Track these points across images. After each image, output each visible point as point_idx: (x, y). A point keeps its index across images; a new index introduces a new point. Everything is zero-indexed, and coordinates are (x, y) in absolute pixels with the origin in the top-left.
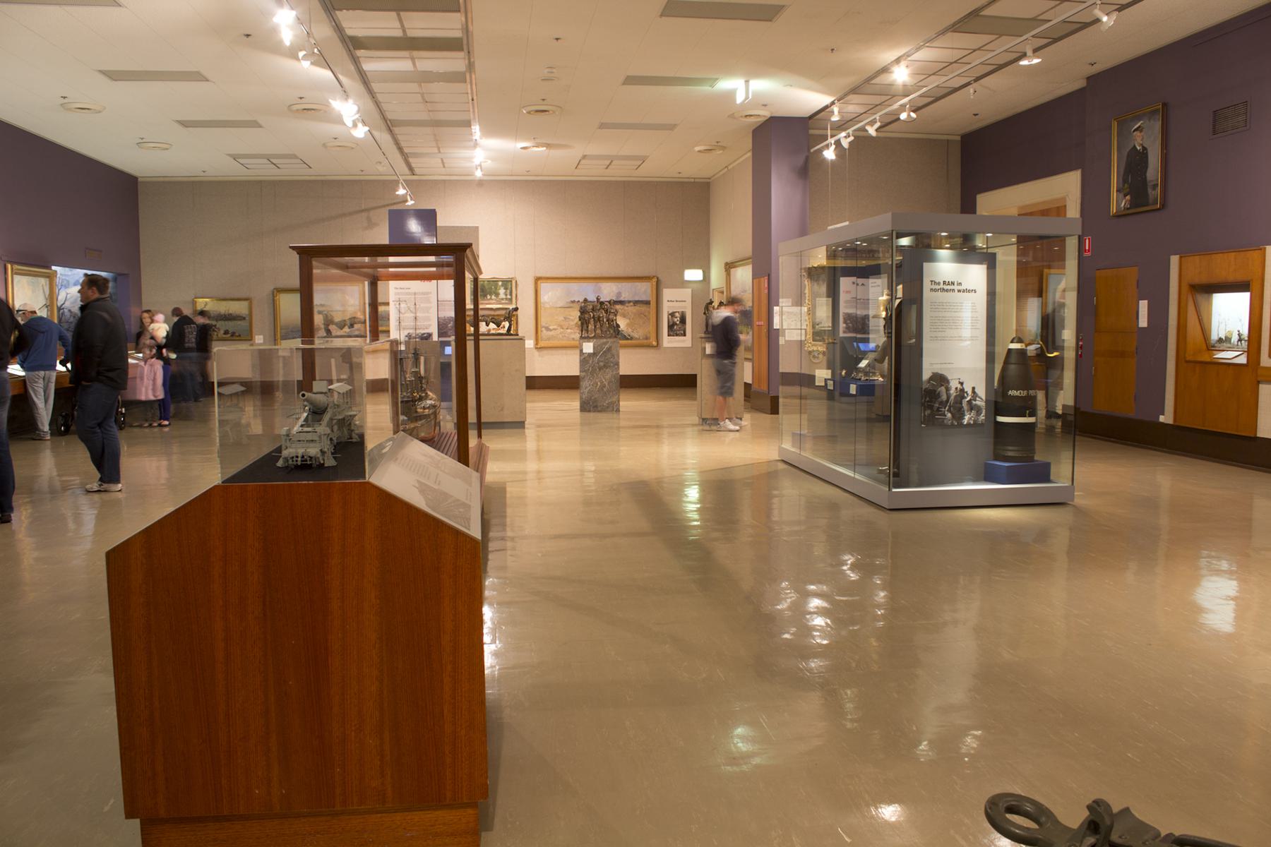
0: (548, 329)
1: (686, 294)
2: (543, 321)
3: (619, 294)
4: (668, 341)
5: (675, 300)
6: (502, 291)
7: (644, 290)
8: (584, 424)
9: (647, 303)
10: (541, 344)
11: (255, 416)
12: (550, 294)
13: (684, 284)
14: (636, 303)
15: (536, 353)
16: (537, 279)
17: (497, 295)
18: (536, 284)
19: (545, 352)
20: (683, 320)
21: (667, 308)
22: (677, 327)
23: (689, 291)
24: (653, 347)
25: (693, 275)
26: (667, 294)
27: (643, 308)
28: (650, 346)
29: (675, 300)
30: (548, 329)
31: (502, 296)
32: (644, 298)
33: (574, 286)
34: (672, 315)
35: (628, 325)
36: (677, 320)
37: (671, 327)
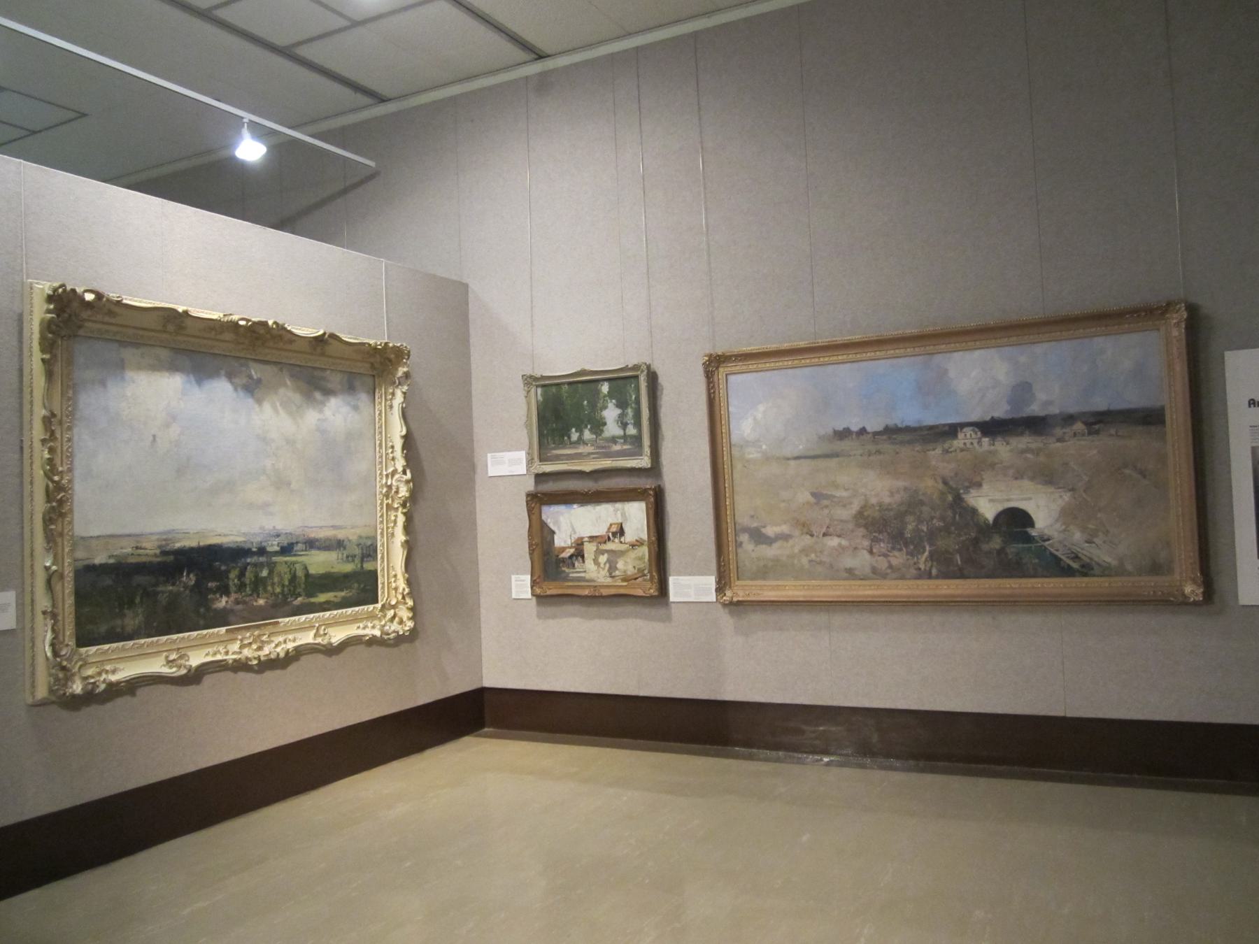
0: (759, 537)
2: (744, 507)
3: (1022, 390)
6: (611, 413)
9: (1151, 418)
10: (740, 591)
12: (764, 413)
14: (1098, 421)
15: (726, 620)
16: (714, 364)
17: (598, 426)
18: (709, 375)
19: (756, 617)
24: (1183, 604)
27: (1134, 442)
28: (1170, 603)
30: (759, 537)
31: (612, 429)
32: (1133, 398)
33: (845, 375)
35: (1068, 515)
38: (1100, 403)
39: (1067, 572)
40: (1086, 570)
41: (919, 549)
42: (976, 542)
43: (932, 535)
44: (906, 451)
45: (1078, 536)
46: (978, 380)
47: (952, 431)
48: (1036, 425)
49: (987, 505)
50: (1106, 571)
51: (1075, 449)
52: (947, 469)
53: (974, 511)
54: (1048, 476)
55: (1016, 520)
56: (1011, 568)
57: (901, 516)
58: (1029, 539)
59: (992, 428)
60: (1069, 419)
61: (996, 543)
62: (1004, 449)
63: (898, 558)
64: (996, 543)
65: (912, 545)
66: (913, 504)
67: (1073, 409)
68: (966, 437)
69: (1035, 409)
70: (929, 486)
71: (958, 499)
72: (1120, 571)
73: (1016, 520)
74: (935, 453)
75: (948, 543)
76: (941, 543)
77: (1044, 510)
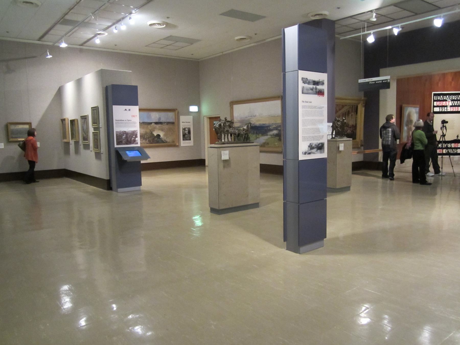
1: (190, 118)
3: (160, 118)
4: (183, 143)
5: (185, 121)
7: (170, 116)
8: (261, 176)
9: (173, 123)
11: (437, 132)
13: (189, 113)
14: (168, 123)
20: (189, 132)
21: (182, 126)
22: (186, 137)
23: (191, 117)
25: (194, 109)
26: (183, 118)
27: (171, 126)
29: (185, 121)
34: (184, 129)
35: (164, 135)
36: (187, 132)
37: (184, 136)
38: (168, 121)
39: (164, 143)
40: (166, 142)
41: (146, 140)
42: (154, 139)
43: (148, 138)
44: (146, 126)
45: (165, 138)
46: (155, 116)
47: (151, 123)
48: (161, 123)
49: (155, 134)
50: (169, 142)
51: (166, 127)
52: (150, 128)
53: (154, 135)
54: (162, 130)
55: (159, 136)
56: (158, 142)
57: (144, 135)
58: (160, 138)
59: (156, 123)
60: (165, 123)
61: (156, 139)
62: (157, 126)
63: (144, 141)
64: (156, 139)
65: (146, 139)
66: (146, 133)
67: (165, 121)
68: (153, 124)
69: (161, 121)
70: (148, 131)
71: (152, 133)
72: (169, 142)
73: (159, 136)
74: (149, 126)
75: (151, 139)
76: (150, 139)
77: (162, 134)
